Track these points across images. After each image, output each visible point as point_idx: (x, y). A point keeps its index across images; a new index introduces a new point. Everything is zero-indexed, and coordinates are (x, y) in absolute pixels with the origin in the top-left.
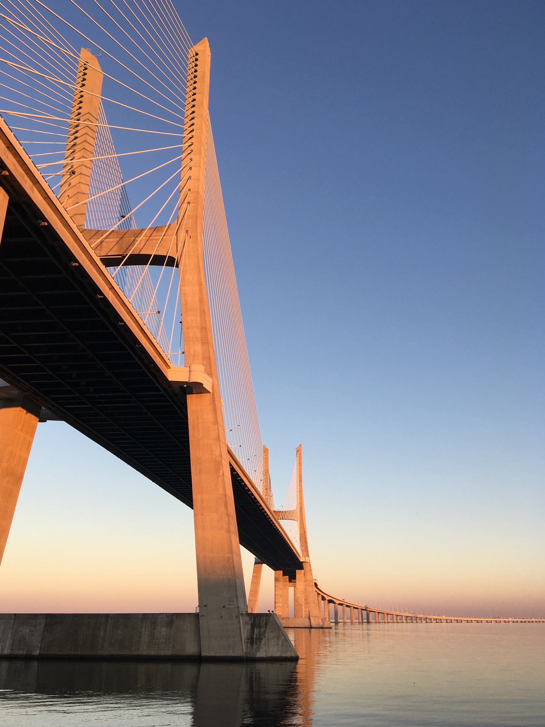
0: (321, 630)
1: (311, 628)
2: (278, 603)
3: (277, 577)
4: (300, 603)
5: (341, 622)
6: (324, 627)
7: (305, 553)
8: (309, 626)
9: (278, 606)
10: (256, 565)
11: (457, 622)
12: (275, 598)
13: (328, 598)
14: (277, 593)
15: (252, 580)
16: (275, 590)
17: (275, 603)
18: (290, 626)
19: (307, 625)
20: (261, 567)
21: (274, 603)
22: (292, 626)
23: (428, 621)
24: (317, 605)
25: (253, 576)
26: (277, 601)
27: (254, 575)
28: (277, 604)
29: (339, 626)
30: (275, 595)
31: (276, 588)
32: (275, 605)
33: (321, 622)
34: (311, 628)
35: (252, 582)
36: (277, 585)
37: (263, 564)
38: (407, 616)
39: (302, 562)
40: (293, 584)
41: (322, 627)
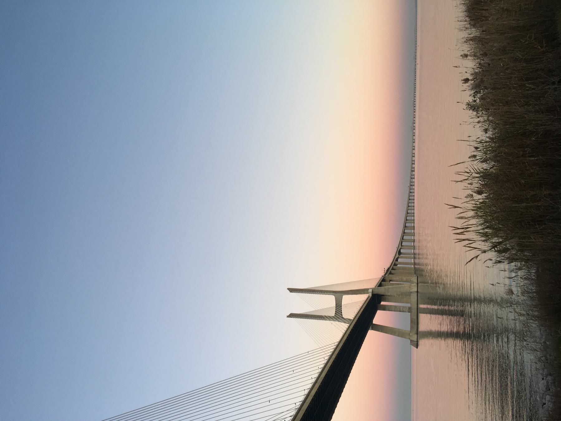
0: (419, 285)
2: (400, 309)
5: (414, 260)
6: (416, 282)
9: (403, 309)
12: (397, 311)
13: (397, 256)
14: (393, 310)
16: (391, 311)
17: (400, 311)
18: (416, 307)
19: (416, 294)
21: (401, 312)
22: (416, 305)
24: (402, 286)
25: (381, 332)
26: (399, 310)
27: (380, 331)
28: (401, 310)
29: (416, 252)
30: (395, 311)
32: (402, 312)
33: (413, 284)
34: (417, 292)
35: (386, 333)
39: (372, 295)
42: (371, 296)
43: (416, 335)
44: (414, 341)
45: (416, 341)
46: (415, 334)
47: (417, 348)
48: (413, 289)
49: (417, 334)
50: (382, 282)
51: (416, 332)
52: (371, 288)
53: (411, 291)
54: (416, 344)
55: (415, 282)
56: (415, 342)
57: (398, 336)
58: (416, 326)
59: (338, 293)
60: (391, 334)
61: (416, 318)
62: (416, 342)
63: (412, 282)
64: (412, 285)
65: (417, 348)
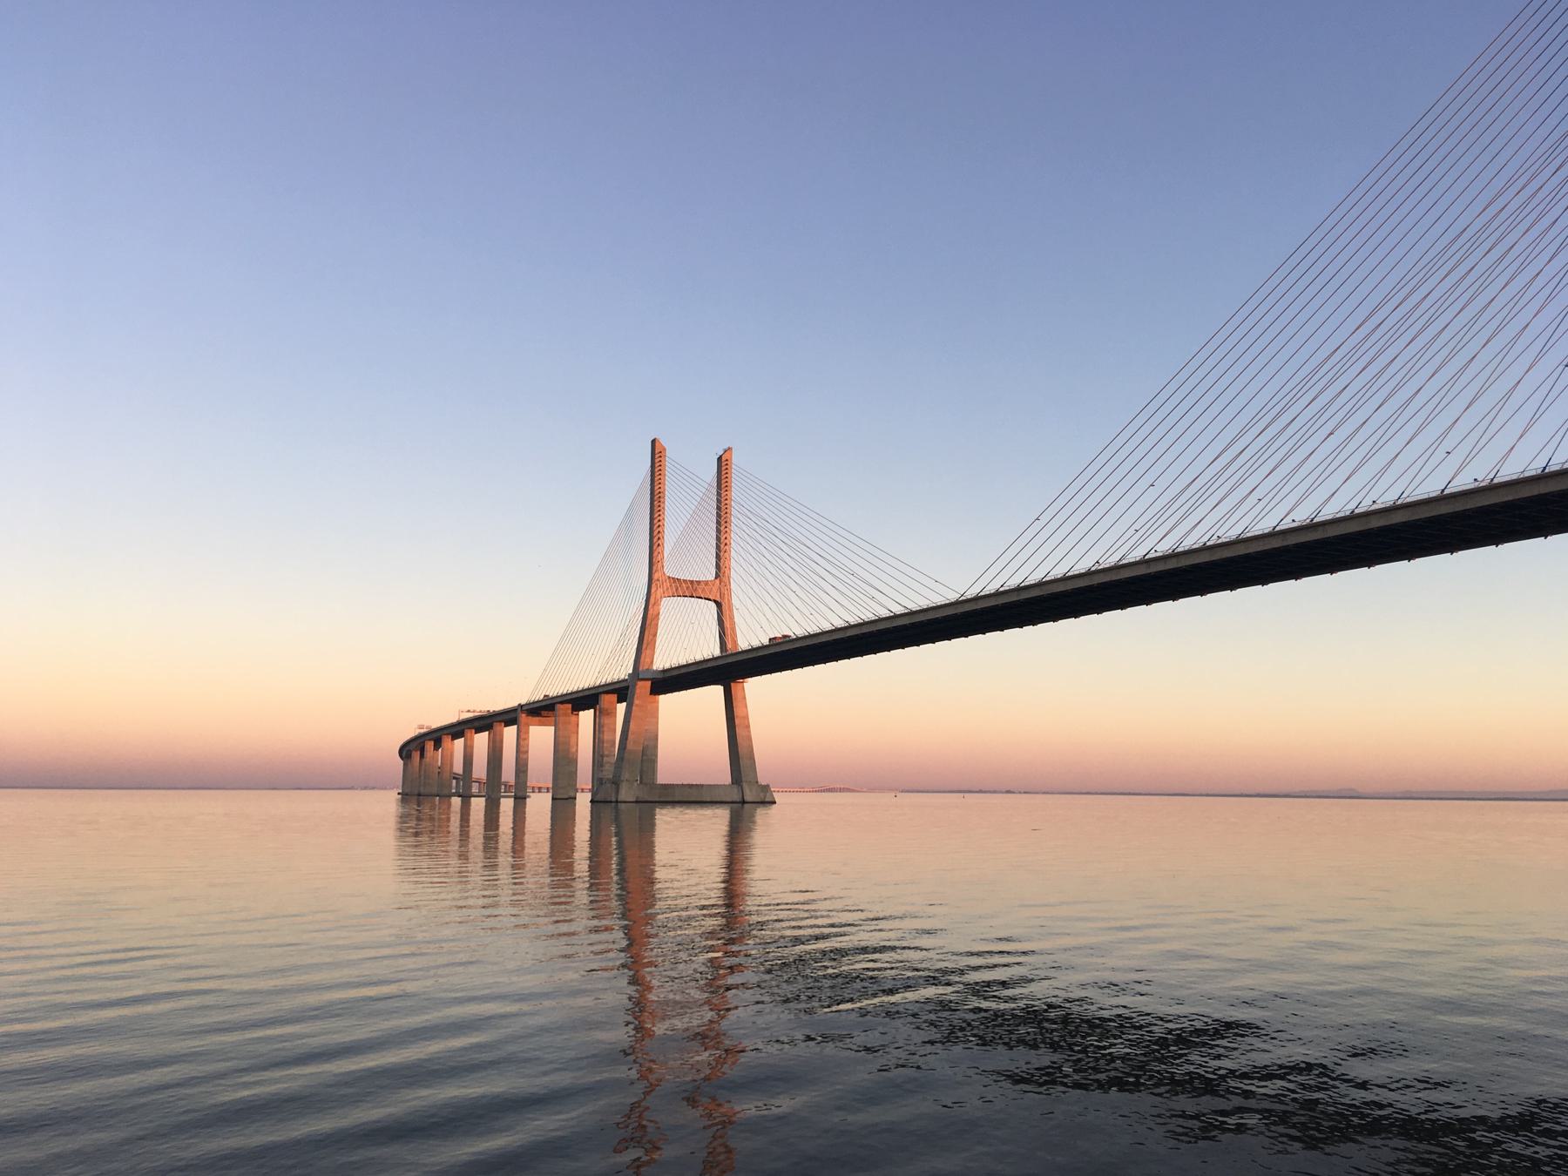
2: (607, 756)
6: (767, 800)
8: (741, 800)
9: (609, 762)
18: (704, 800)
22: (708, 800)
28: (605, 759)
34: (744, 802)
41: (763, 800)
43: (634, 800)
44: (617, 792)
45: (619, 800)
46: (637, 798)
48: (751, 791)
49: (636, 802)
53: (745, 785)
54: (609, 800)
56: (613, 795)
58: (657, 799)
61: (676, 799)
62: (614, 799)
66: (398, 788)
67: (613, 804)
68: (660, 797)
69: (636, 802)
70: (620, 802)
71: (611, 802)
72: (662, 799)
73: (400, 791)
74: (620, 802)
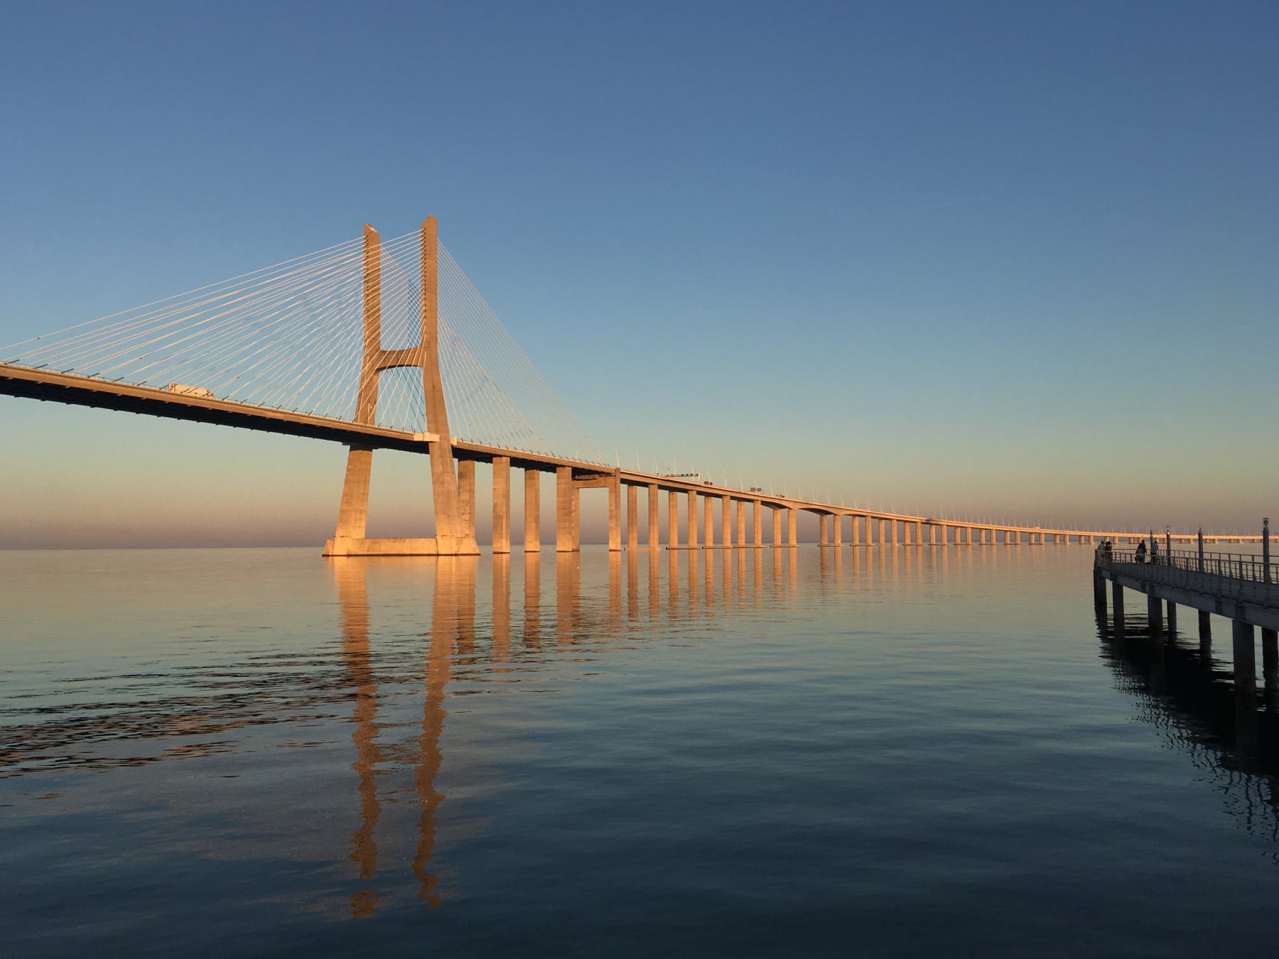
1: (438, 555)
3: (461, 470)
4: (499, 514)
7: (432, 426)
10: (352, 452)
11: (1181, 542)
15: (347, 475)
20: (371, 455)
22: (408, 553)
23: (1132, 542)
27: (350, 467)
31: (461, 491)
34: (438, 555)
35: (346, 482)
36: (461, 484)
37: (373, 450)
38: (1030, 533)
40: (584, 484)
42: (418, 438)
43: (345, 554)
45: (334, 554)
47: (323, 556)
49: (349, 556)
50: (571, 469)
51: (352, 553)
52: (445, 438)
55: (459, 548)
57: (342, 511)
58: (366, 553)
59: (427, 354)
60: (345, 495)
61: (381, 553)
62: (330, 554)
63: (460, 540)
64: (454, 542)
65: (323, 556)
66: (815, 542)
67: (330, 557)
68: (368, 551)
69: (349, 556)
70: (335, 556)
71: (328, 556)
72: (369, 553)
73: (819, 544)
74: (335, 556)
